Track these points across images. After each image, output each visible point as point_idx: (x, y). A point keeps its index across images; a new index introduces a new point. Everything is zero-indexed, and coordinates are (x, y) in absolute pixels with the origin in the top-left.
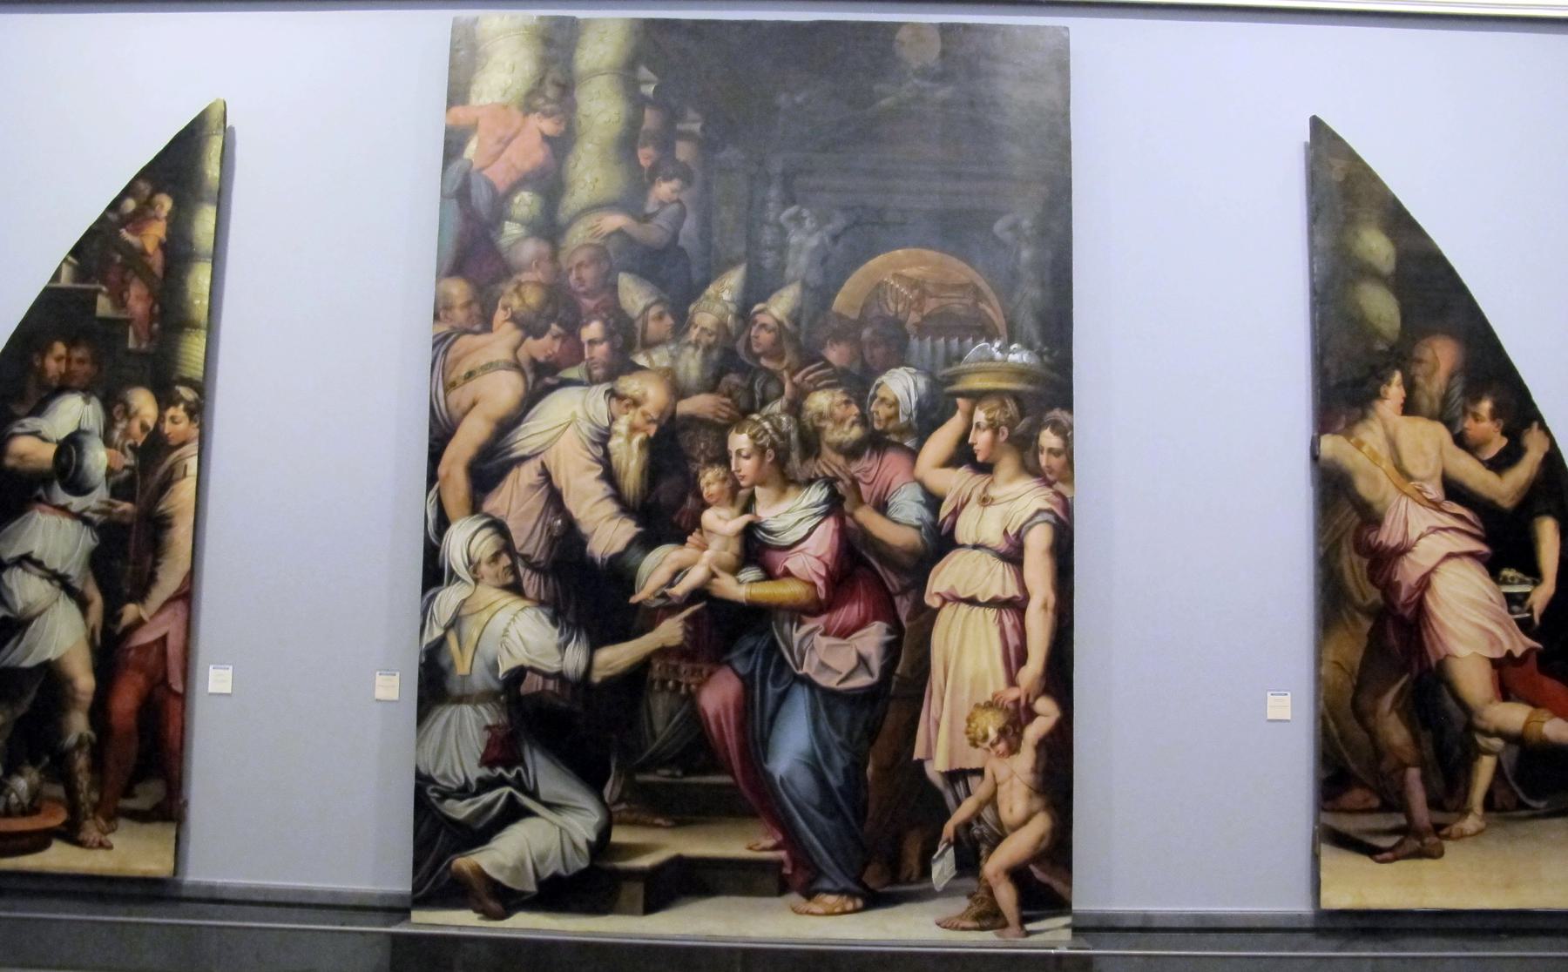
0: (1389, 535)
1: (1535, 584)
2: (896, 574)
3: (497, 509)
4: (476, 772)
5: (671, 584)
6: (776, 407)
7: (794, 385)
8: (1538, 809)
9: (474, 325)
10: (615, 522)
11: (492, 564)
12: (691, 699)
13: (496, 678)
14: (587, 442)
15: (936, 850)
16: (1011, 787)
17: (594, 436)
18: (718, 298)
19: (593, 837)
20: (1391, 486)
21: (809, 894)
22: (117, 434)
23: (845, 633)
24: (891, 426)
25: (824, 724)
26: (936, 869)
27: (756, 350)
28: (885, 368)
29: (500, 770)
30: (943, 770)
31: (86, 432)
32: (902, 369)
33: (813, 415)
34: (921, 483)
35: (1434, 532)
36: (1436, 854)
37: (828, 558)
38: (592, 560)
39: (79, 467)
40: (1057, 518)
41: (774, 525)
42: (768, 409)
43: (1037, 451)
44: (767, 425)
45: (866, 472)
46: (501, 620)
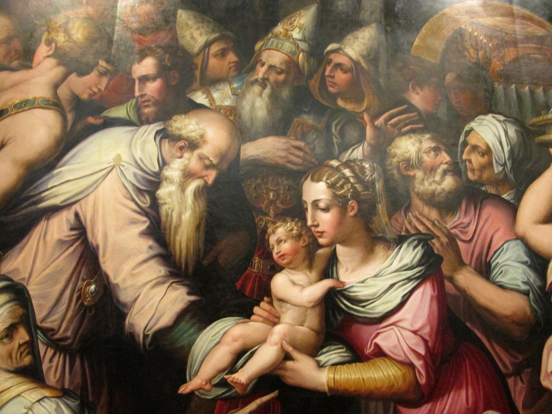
3: (16, 270)
5: (232, 368)
6: (358, 153)
7: (375, 128)
9: (11, 61)
10: (162, 289)
11: (5, 340)
17: (138, 181)
18: (288, 37)
24: (485, 176)
33: (399, 162)
37: (427, 330)
38: (132, 336)
41: (361, 292)
42: (346, 156)
44: (347, 172)
45: (464, 228)
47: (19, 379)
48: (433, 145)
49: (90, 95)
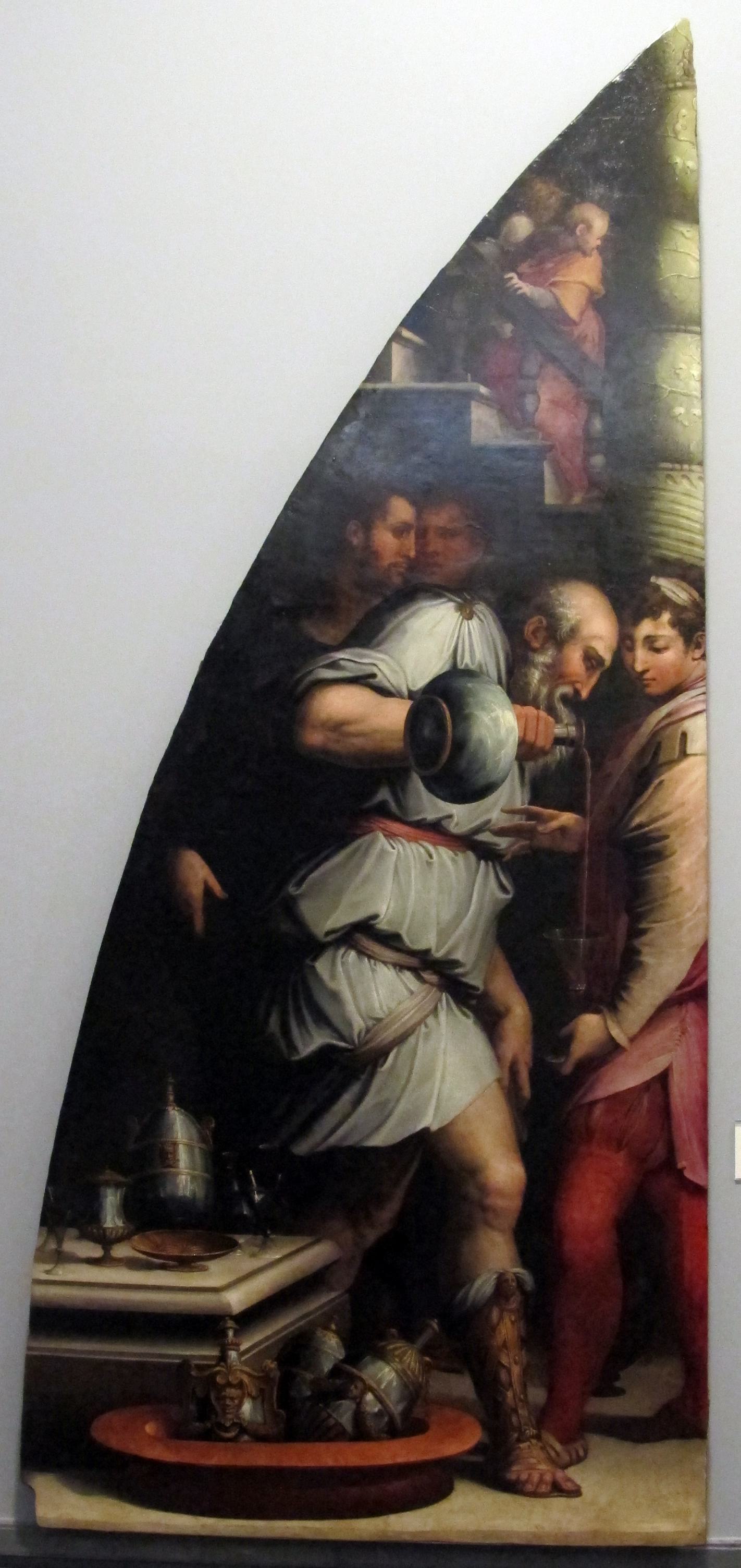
22: (536, 675)
31: (469, 674)
39: (460, 745)
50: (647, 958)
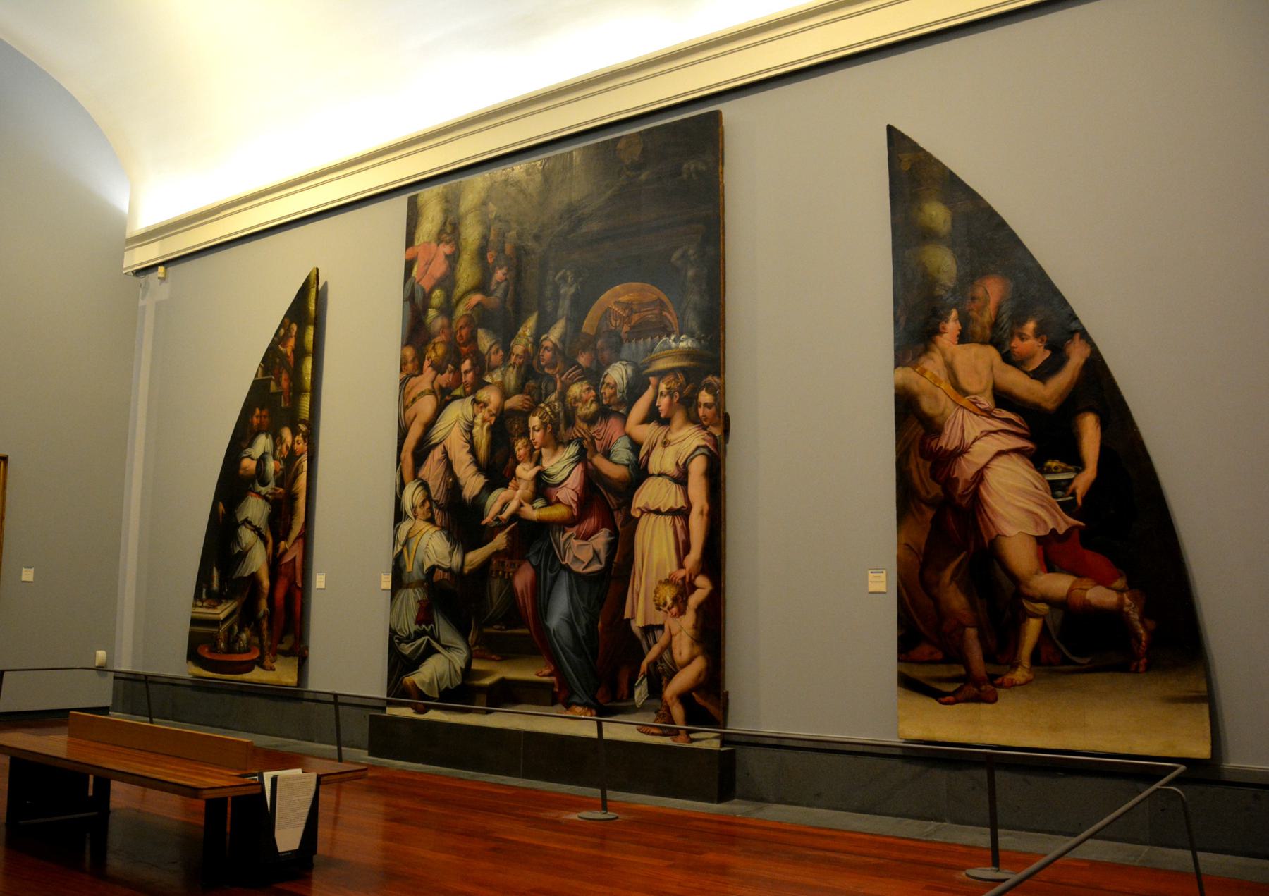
0: (949, 440)
1: (1078, 471)
2: (615, 497)
3: (424, 475)
4: (414, 627)
5: (501, 512)
6: (553, 397)
7: (562, 382)
8: (1084, 665)
12: (509, 581)
13: (423, 572)
14: (462, 430)
15: (637, 679)
16: (680, 639)
18: (524, 335)
19: (463, 667)
20: (950, 404)
21: (568, 706)
22: (278, 452)
23: (586, 537)
24: (612, 400)
25: (576, 596)
26: (637, 692)
27: (543, 363)
28: (609, 365)
29: (424, 626)
30: (641, 626)
32: (618, 363)
34: (629, 435)
35: (985, 436)
36: (992, 700)
37: (578, 488)
39: (265, 471)
40: (710, 451)
41: (551, 471)
42: (548, 400)
43: (698, 405)
44: (548, 409)
46: (426, 538)
47: (428, 524)
48: (588, 386)
49: (447, 385)
50: (293, 526)
